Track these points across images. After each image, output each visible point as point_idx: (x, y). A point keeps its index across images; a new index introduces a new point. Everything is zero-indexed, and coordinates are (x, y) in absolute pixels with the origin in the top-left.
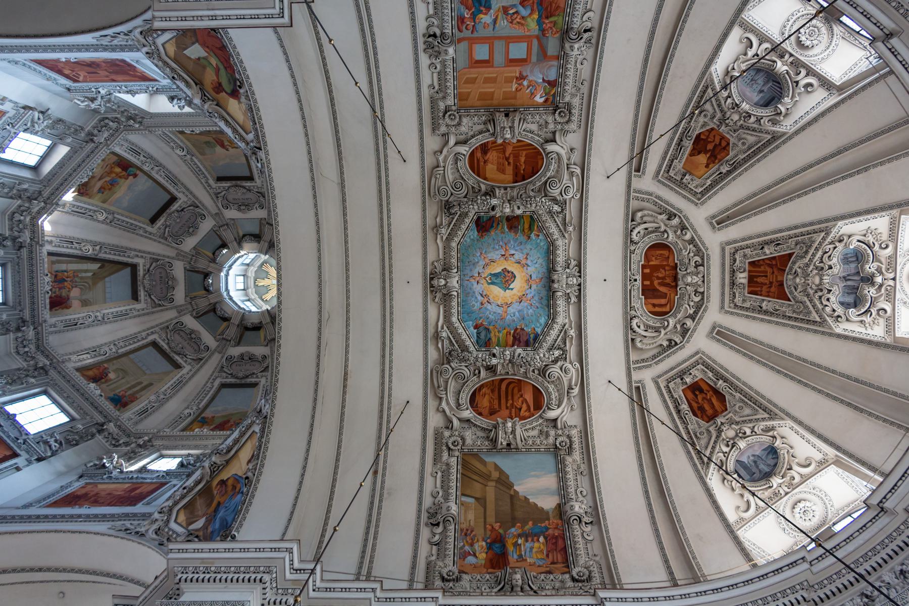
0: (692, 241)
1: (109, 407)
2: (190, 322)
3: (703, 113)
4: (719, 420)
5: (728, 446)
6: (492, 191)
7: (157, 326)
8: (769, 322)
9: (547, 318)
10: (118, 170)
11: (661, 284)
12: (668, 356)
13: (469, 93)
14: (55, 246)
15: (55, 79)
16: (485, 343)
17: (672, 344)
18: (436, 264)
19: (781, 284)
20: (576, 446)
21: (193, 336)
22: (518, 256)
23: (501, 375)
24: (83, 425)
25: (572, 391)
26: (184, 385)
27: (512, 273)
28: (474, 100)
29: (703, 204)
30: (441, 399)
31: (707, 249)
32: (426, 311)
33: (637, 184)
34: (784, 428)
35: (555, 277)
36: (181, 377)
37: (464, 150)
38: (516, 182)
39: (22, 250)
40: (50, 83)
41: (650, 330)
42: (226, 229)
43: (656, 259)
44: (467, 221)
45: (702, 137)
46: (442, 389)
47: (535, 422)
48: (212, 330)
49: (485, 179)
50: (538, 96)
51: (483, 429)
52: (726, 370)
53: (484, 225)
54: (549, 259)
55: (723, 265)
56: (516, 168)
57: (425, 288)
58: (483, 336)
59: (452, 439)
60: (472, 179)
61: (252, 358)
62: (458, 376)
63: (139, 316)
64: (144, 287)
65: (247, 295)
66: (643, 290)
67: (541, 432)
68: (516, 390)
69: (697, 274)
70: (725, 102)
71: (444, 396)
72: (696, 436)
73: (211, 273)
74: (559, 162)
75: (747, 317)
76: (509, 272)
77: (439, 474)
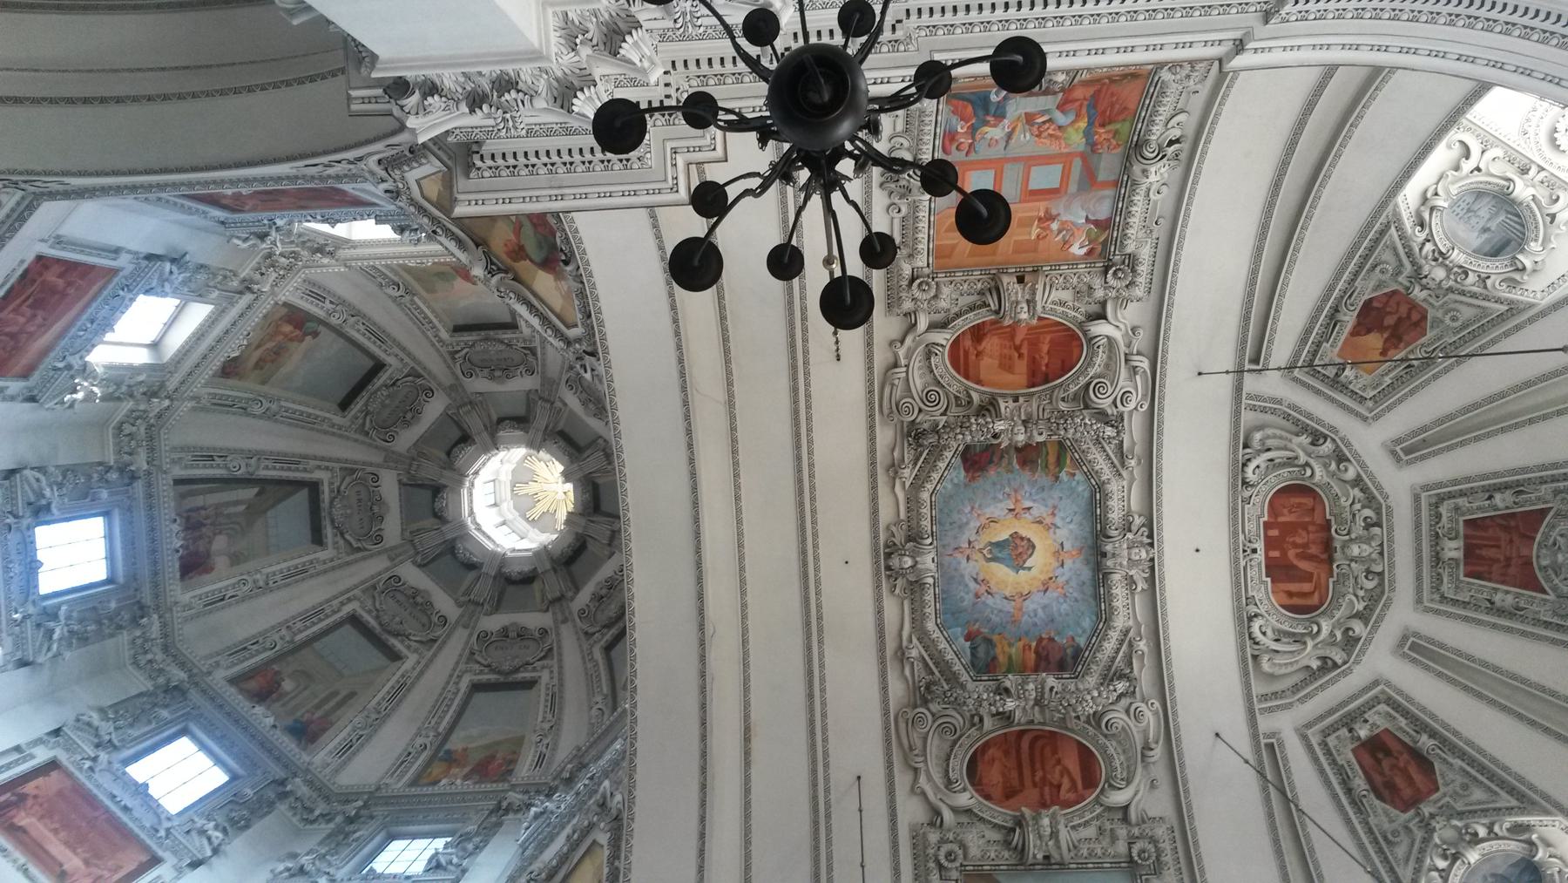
0: (1357, 482)
1: (287, 744)
2: (412, 575)
3: (1378, 269)
4: (1426, 810)
5: (1445, 857)
6: (991, 404)
8: (1509, 630)
9: (1094, 618)
10: (287, 328)
11: (1299, 556)
12: (1322, 687)
14: (186, 467)
15: (204, 212)
16: (985, 665)
17: (1327, 665)
18: (894, 529)
19: (1528, 563)
20: (1168, 858)
21: (419, 599)
22: (1039, 510)
23: (1019, 724)
24: (252, 787)
25: (1151, 753)
26: (409, 690)
27: (1029, 540)
29: (1377, 418)
30: (916, 770)
31: (1386, 497)
32: (879, 612)
33: (1251, 383)
34: (1550, 828)
35: (1109, 548)
36: (403, 676)
37: (943, 338)
38: (1033, 386)
39: (135, 485)
40: (195, 217)
41: (1284, 640)
42: (469, 412)
43: (1290, 512)
44: (948, 454)
45: (1375, 304)
46: (916, 752)
47: (1087, 810)
48: (450, 587)
49: (979, 382)
52: (1433, 716)
53: (977, 460)
54: (1093, 513)
55: (1418, 525)
57: (877, 574)
59: (945, 848)
60: (955, 383)
61: (522, 634)
62: (945, 729)
63: (325, 572)
64: (333, 521)
65: (500, 514)
66: (1267, 567)
67: (1101, 830)
68: (1048, 750)
69: (1368, 540)
70: (1421, 249)
72: (1385, 839)
73: (445, 486)
74: (1110, 351)
75: (1466, 619)
76: (1022, 539)
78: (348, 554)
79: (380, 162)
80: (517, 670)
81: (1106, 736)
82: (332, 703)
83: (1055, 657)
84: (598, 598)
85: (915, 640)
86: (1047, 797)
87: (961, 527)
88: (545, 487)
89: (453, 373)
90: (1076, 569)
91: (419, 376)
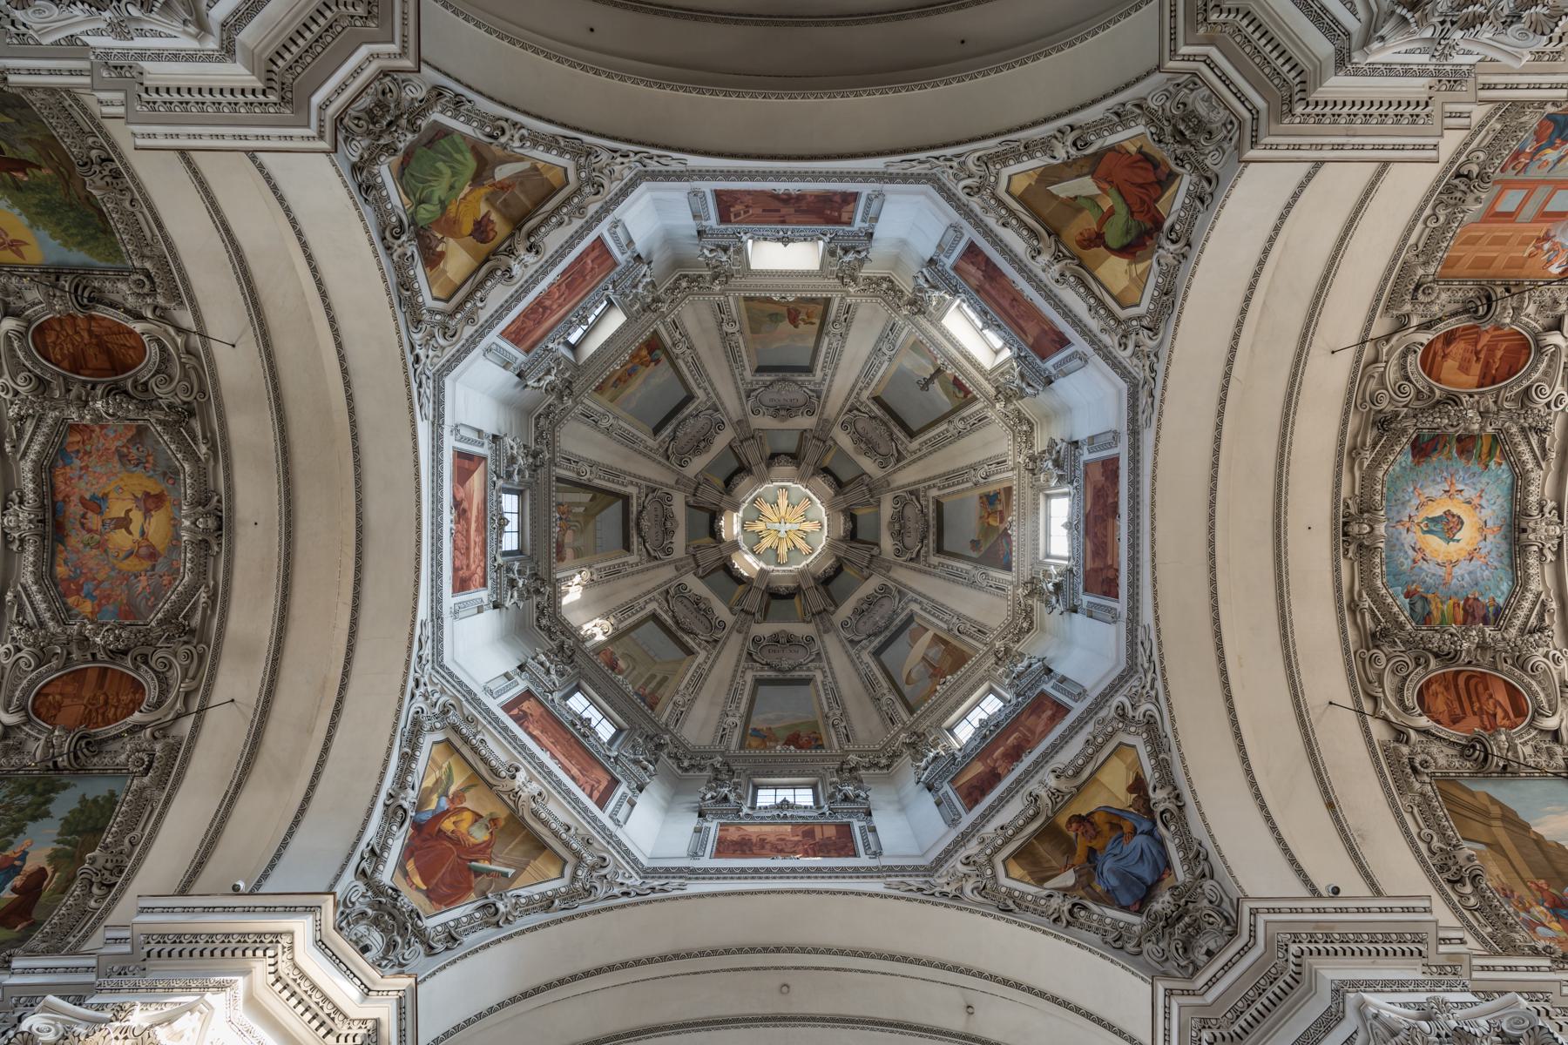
2: (696, 586)
7: (655, 589)
13: (1460, 258)
18: (1350, 502)
22: (1469, 493)
32: (1337, 570)
38: (1482, 386)
48: (724, 598)
49: (1438, 380)
50: (1556, 265)
53: (1423, 449)
56: (1487, 365)
57: (1335, 537)
60: (1420, 379)
68: (1481, 688)
76: (1453, 516)
77: (1416, 810)
80: (793, 669)
81: (1531, 676)
82: (652, 685)
84: (859, 612)
85: (1365, 595)
86: (1487, 723)
88: (770, 526)
90: (1494, 544)
91: (717, 410)
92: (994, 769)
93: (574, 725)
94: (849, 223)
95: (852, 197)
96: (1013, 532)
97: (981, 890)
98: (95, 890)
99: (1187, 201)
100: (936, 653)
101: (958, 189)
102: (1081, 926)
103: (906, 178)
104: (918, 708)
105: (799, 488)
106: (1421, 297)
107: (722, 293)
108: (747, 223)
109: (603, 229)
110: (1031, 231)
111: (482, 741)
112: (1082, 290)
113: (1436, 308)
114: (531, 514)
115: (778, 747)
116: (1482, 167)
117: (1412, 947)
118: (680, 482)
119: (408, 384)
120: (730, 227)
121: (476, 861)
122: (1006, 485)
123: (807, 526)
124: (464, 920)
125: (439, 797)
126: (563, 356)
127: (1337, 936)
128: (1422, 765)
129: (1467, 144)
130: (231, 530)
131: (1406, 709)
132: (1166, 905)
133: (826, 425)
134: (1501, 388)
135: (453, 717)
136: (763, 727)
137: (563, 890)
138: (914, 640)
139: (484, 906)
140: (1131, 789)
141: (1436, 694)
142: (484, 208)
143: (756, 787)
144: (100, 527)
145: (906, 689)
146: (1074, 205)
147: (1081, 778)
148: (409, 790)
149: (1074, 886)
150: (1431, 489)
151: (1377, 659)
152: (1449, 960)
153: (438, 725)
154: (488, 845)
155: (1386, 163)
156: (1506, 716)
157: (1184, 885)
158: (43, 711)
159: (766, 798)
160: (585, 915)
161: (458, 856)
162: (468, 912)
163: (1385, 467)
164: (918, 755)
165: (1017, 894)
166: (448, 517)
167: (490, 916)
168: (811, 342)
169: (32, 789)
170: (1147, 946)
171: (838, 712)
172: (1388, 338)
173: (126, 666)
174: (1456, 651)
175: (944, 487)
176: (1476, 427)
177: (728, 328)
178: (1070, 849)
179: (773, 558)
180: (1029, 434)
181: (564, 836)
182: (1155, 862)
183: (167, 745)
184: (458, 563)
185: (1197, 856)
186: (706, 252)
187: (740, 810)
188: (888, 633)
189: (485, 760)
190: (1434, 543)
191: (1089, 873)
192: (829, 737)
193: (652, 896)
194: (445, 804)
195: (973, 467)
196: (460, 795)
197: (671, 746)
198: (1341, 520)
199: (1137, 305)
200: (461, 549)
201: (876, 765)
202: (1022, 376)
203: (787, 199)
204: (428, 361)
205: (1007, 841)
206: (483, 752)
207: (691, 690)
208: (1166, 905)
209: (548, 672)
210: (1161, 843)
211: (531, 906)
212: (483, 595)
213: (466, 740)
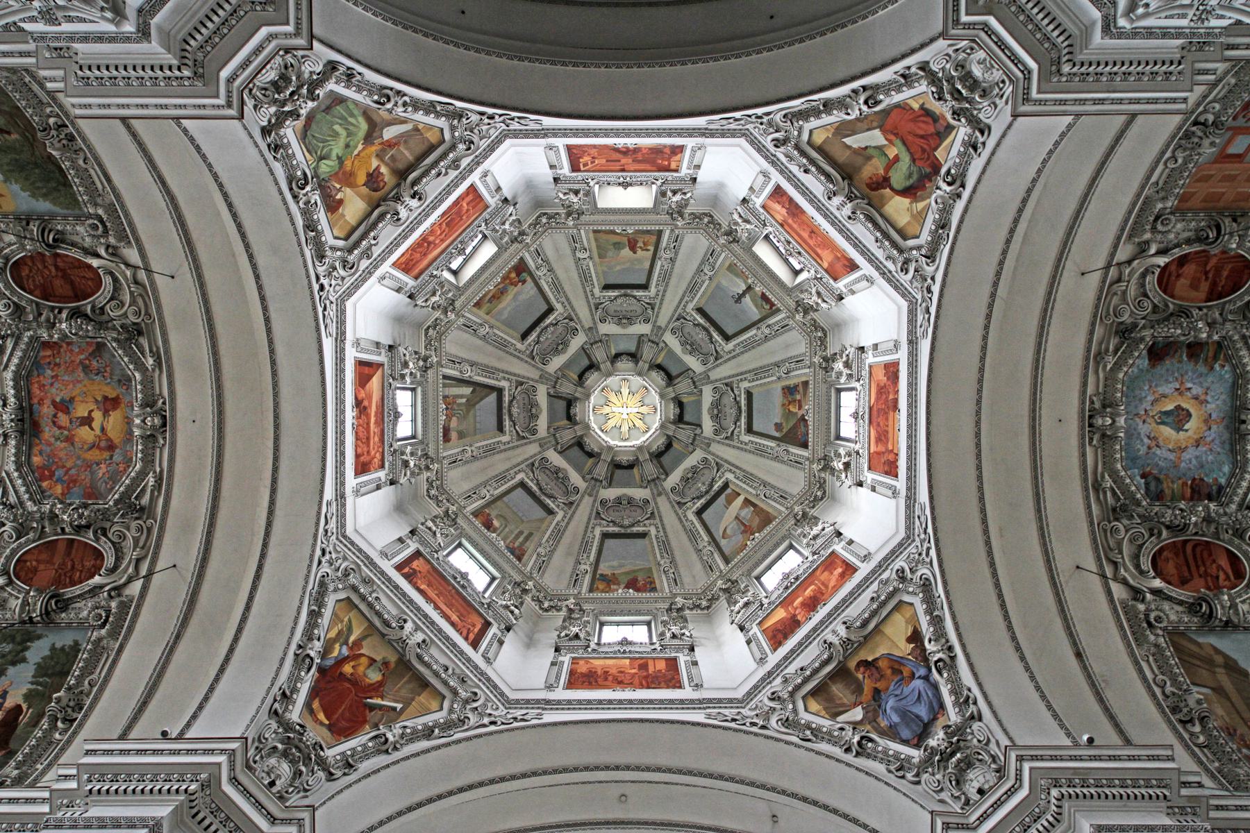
7: (522, 462)
13: (1194, 193)
18: (1095, 399)
22: (1197, 390)
27: (1188, 411)
28: (1195, 202)
32: (1083, 455)
48: (579, 469)
49: (1172, 296)
51: (1181, 603)
53: (1157, 354)
56: (1214, 284)
57: (1082, 428)
58: (1153, 486)
63: (505, 450)
68: (1205, 554)
71: (1120, 560)
76: (1183, 409)
77: (1151, 659)
78: (517, 440)
79: (784, 117)
80: (633, 525)
82: (521, 539)
83: (1205, 491)
84: (685, 480)
85: (1107, 477)
86: (1211, 584)
87: (1141, 400)
88: (614, 409)
89: (593, 319)
90: (1217, 432)
91: (571, 320)
92: (795, 616)
93: (455, 578)
94: (676, 171)
95: (681, 149)
96: (809, 418)
97: (786, 722)
98: (60, 724)
99: (962, 149)
100: (747, 513)
101: (768, 142)
102: (868, 756)
103: (723, 134)
104: (733, 560)
105: (637, 381)
106: (1160, 227)
107: (575, 226)
108: (593, 171)
109: (475, 178)
110: (828, 177)
111: (377, 598)
112: (870, 225)
113: (1172, 236)
114: (423, 406)
115: (620, 591)
116: (1217, 116)
117: (1158, 791)
118: (543, 378)
119: (315, 309)
120: (579, 176)
121: (370, 698)
122: (804, 379)
123: (644, 410)
124: (360, 749)
125: (341, 646)
126: (446, 280)
127: (1092, 781)
128: (1156, 620)
129: (1205, 97)
130: (174, 427)
131: (1142, 572)
132: (941, 742)
133: (659, 330)
134: (1225, 303)
135: (352, 579)
136: (608, 572)
137: (442, 721)
138: (729, 501)
139: (375, 737)
140: (909, 640)
141: (1167, 560)
142: (375, 163)
143: (602, 624)
144: (68, 424)
145: (723, 543)
146: (864, 153)
147: (869, 629)
148: (316, 642)
149: (862, 720)
150: (1164, 388)
151: (1117, 530)
152: (1189, 802)
153: (340, 586)
154: (380, 684)
155: (1133, 116)
156: (1228, 578)
157: (956, 725)
158: (22, 574)
159: (611, 634)
160: (459, 741)
161: (356, 695)
162: (362, 742)
163: (1125, 369)
164: (732, 602)
165: (814, 726)
166: (350, 414)
167: (383, 746)
168: (647, 265)
169: (12, 639)
170: (925, 777)
171: (668, 561)
172: (1129, 262)
173: (89, 538)
174: (1185, 524)
175: (753, 380)
176: (1204, 335)
177: (580, 255)
178: (858, 689)
179: (617, 435)
180: (823, 341)
181: (443, 675)
182: (931, 703)
183: (121, 603)
184: (359, 451)
185: (964, 702)
186: (561, 195)
187: (588, 646)
188: (708, 497)
189: (379, 614)
190: (1167, 431)
191: (875, 710)
192: (662, 581)
193: (516, 724)
194: (345, 652)
195: (777, 365)
196: (358, 644)
197: (534, 591)
198: (1087, 414)
199: (918, 237)
200: (362, 438)
201: (698, 606)
202: (819, 294)
203: (626, 152)
204: (331, 289)
205: (806, 680)
206: (378, 607)
207: (551, 543)
208: (941, 742)
209: (435, 533)
210: (935, 687)
211: (415, 736)
212: (382, 474)
213: (363, 598)
